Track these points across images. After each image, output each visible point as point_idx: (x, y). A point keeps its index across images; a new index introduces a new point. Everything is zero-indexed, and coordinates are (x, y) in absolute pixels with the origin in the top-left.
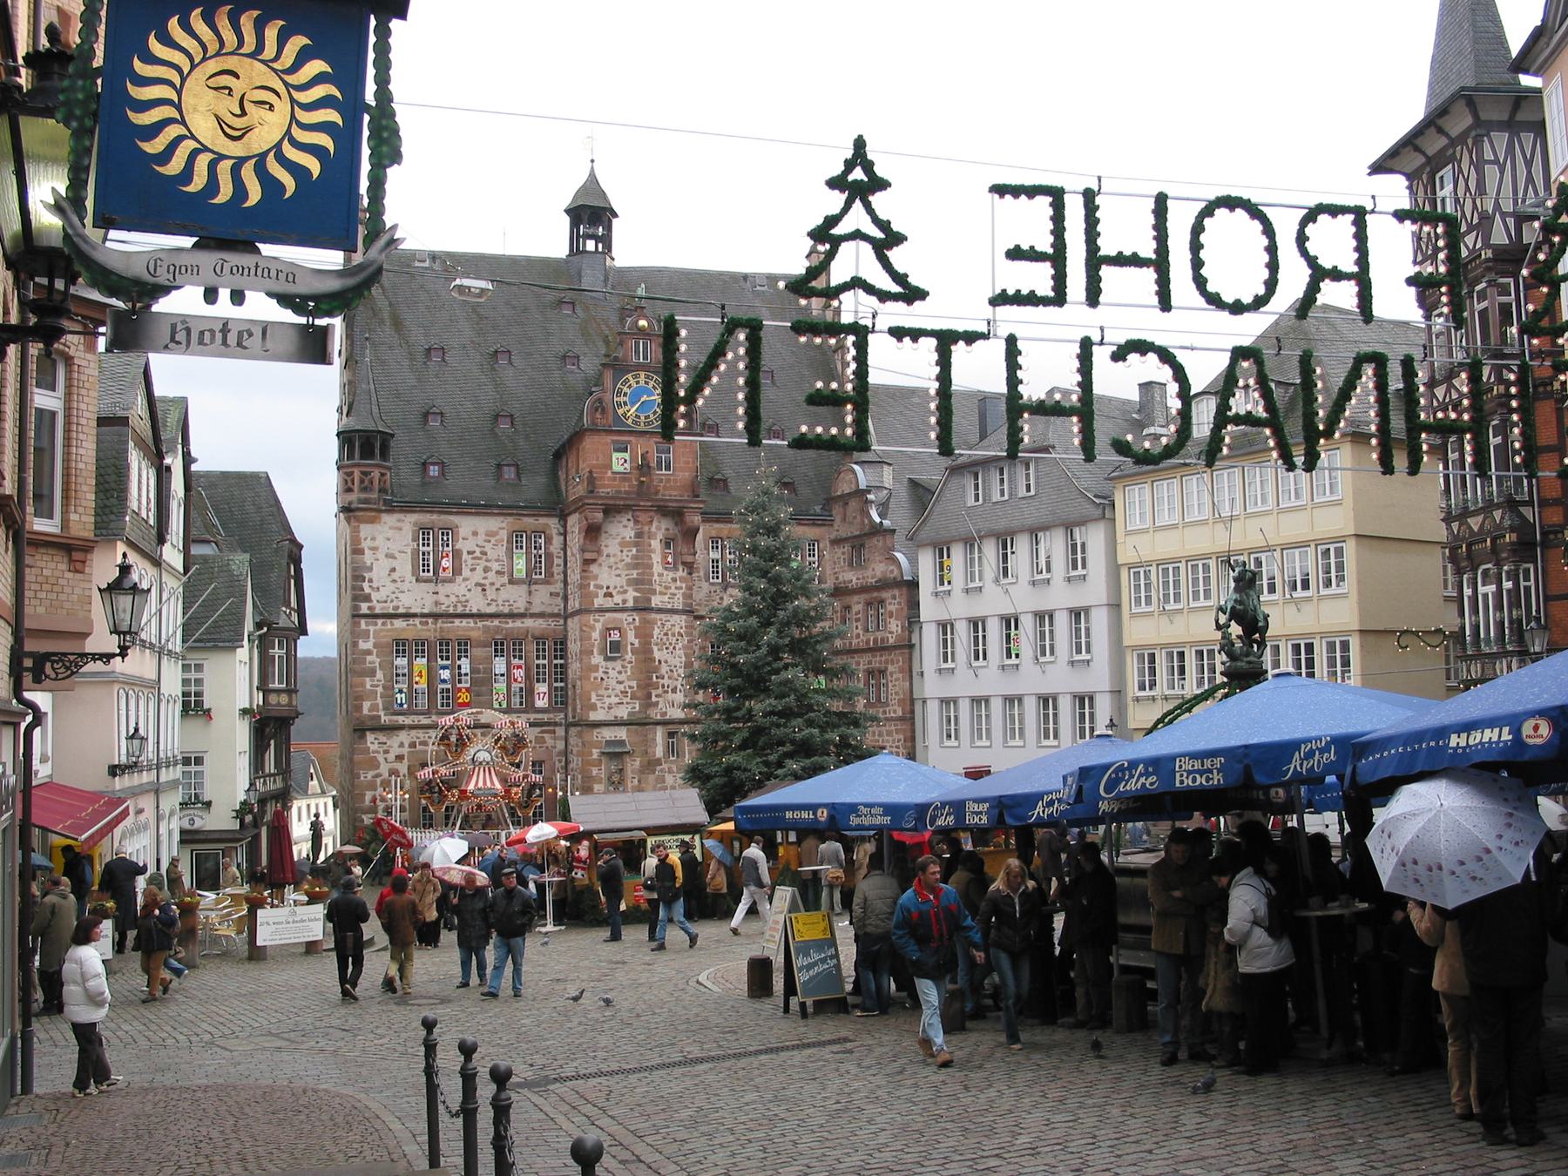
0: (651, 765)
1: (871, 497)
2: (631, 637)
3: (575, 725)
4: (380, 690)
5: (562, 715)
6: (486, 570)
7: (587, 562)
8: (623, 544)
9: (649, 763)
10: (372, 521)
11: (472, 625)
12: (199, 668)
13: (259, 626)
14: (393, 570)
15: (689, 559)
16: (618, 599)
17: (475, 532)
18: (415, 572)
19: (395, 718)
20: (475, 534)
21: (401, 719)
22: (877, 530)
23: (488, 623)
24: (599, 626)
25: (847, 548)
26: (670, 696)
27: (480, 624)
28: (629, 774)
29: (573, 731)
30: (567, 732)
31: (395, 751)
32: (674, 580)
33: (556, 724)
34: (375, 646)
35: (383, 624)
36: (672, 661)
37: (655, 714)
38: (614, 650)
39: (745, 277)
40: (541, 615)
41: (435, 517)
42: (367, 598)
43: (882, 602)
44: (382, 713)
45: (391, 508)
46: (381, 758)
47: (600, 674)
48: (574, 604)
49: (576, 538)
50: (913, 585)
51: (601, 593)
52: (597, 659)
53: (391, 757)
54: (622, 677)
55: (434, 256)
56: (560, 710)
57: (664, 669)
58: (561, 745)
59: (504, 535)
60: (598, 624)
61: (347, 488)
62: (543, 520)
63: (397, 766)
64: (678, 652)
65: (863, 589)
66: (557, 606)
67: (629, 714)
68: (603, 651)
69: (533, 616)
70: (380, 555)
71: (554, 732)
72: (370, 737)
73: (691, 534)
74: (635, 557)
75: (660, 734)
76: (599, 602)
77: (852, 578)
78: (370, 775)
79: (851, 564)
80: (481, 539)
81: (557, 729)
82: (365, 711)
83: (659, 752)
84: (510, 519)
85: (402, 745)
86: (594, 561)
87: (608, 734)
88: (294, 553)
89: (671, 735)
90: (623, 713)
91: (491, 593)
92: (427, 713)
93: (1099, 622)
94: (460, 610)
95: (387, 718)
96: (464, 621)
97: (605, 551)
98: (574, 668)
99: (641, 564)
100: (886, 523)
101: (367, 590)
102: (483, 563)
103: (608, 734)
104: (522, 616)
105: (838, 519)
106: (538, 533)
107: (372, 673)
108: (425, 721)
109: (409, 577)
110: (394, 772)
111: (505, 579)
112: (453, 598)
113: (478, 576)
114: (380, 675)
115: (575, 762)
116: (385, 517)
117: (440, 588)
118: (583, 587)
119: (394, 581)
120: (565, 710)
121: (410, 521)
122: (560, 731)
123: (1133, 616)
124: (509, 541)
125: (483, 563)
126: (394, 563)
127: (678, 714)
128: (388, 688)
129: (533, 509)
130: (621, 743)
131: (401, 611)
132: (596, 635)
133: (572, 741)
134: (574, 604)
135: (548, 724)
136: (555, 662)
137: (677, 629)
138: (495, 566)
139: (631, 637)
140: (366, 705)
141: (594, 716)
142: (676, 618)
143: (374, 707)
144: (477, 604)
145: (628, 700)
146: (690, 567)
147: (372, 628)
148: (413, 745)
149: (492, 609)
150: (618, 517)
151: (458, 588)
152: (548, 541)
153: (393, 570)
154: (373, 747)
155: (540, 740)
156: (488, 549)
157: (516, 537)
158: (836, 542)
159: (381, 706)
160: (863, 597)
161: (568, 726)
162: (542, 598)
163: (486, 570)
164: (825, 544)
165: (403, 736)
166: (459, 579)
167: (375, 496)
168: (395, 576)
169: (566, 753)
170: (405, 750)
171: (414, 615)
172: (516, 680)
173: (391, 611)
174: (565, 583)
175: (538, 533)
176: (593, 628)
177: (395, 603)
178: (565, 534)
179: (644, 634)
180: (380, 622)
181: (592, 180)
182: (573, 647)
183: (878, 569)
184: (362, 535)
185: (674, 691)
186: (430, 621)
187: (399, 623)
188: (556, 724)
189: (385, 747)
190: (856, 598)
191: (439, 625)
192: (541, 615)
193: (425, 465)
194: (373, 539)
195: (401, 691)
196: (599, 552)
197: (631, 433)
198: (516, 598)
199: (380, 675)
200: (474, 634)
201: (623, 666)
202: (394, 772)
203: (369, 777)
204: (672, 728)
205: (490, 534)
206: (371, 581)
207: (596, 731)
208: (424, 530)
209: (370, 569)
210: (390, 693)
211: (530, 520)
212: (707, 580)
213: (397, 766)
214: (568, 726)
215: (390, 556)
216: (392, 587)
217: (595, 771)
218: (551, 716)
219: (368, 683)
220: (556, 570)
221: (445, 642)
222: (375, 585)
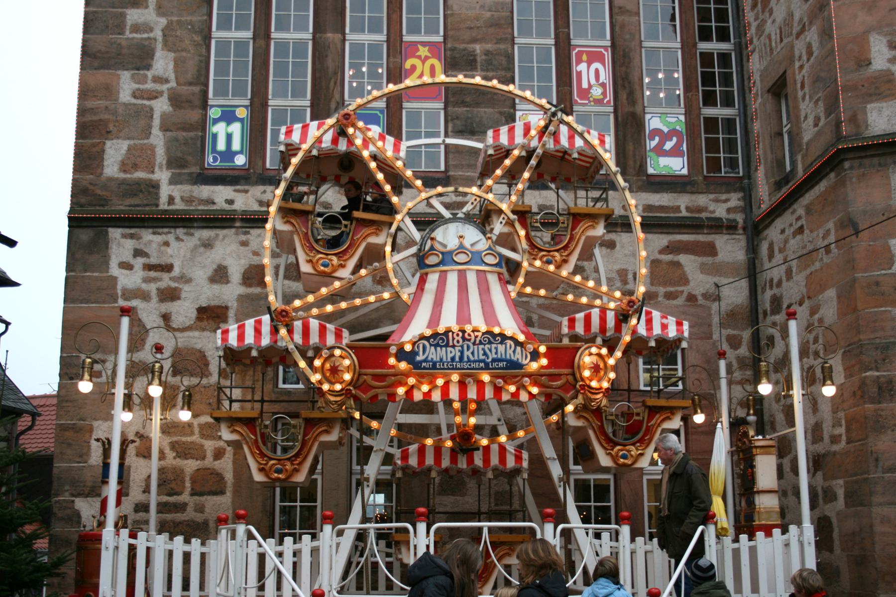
4: (161, 106)
5: (735, 200)
19: (205, 191)
30: (753, 249)
33: (717, 226)
44: (162, 176)
56: (729, 185)
71: (710, 250)
81: (721, 241)
85: (220, 275)
95: (178, 191)
120: (746, 187)
133: (773, 271)
135: (693, 225)
136: (704, 46)
154: (128, 280)
172: (585, 93)
188: (717, 226)
189: (166, 281)
195: (229, 117)
210: (194, 115)
218: (702, 200)
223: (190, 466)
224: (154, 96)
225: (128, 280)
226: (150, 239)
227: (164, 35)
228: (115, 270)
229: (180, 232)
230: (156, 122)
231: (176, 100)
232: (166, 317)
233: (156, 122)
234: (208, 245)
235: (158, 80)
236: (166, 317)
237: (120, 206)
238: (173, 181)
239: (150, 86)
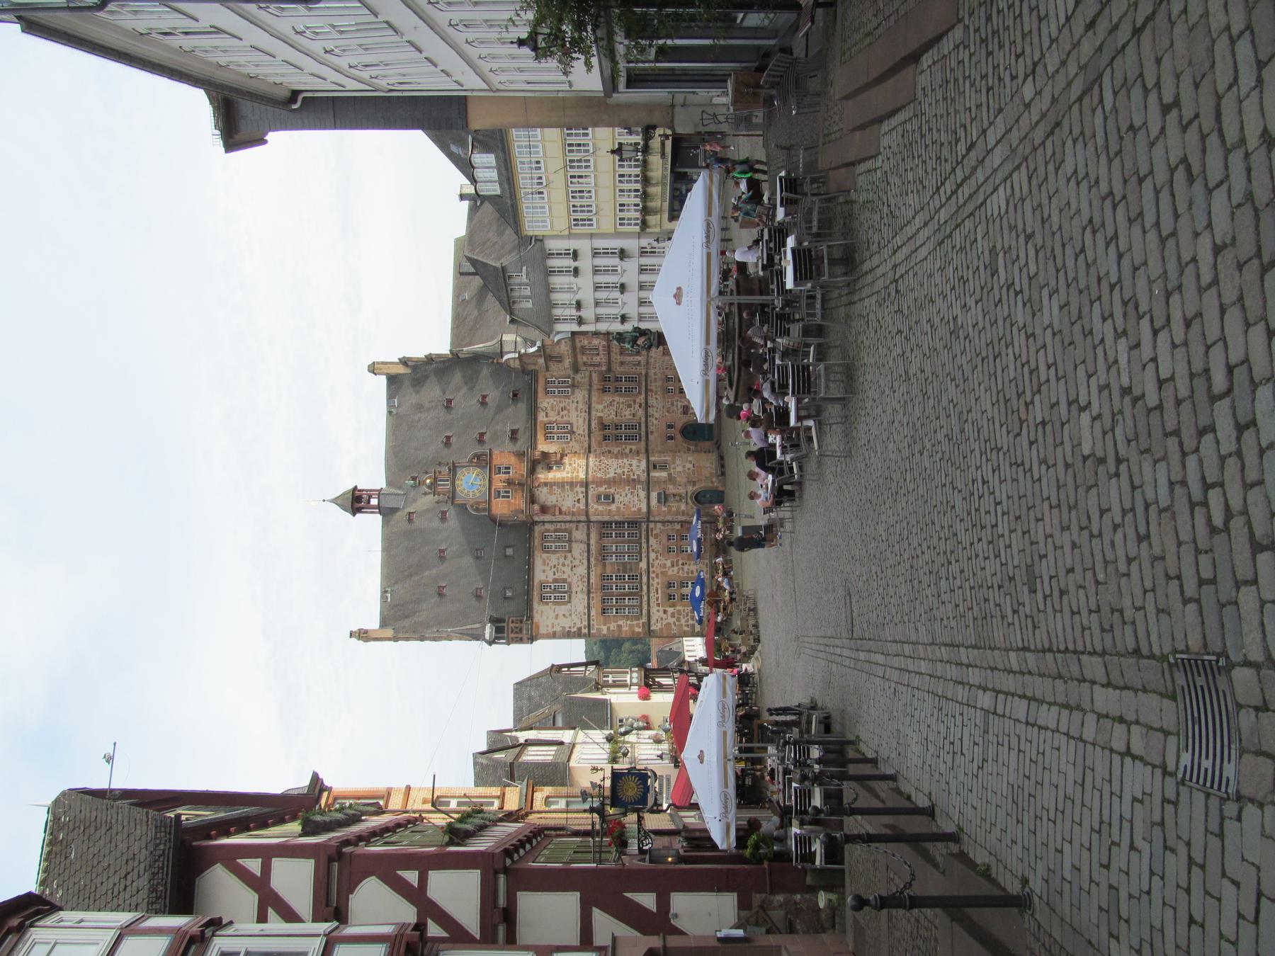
0: (671, 479)
1: (523, 351)
2: (602, 489)
3: (648, 518)
6: (564, 565)
7: (561, 512)
8: (551, 493)
9: (670, 480)
10: (538, 627)
12: (621, 721)
13: (597, 689)
15: (559, 456)
16: (581, 496)
17: (545, 569)
18: (565, 603)
20: (544, 571)
21: (644, 611)
22: (543, 347)
24: (595, 506)
25: (551, 364)
26: (634, 467)
28: (676, 491)
29: (651, 519)
32: (570, 464)
33: (648, 527)
36: (615, 466)
37: (643, 477)
38: (609, 498)
39: (390, 413)
40: (588, 535)
41: (535, 593)
42: (580, 629)
43: (583, 347)
45: (530, 617)
46: (665, 622)
47: (622, 506)
48: (583, 518)
49: (547, 518)
50: (573, 333)
51: (577, 505)
52: (613, 507)
53: (665, 616)
55: (384, 592)
57: (619, 471)
58: (659, 525)
59: (545, 556)
60: (594, 507)
61: (521, 641)
62: (536, 534)
63: (669, 614)
64: (610, 463)
65: (575, 356)
66: (583, 526)
68: (609, 504)
69: (589, 540)
70: (556, 622)
73: (545, 455)
74: (558, 487)
75: (654, 474)
76: (582, 506)
77: (567, 362)
79: (560, 361)
80: (547, 568)
82: (640, 630)
83: (664, 474)
84: (536, 552)
86: (560, 509)
87: (654, 502)
88: (556, 669)
89: (655, 467)
90: (643, 494)
91: (576, 562)
92: (641, 597)
93: (601, 244)
94: (586, 580)
97: (555, 503)
98: (617, 518)
99: (562, 484)
100: (539, 344)
101: (575, 629)
102: (560, 567)
103: (654, 502)
104: (589, 545)
105: (533, 367)
106: (544, 537)
107: (620, 626)
108: (645, 599)
110: (673, 615)
111: (569, 555)
112: (580, 583)
113: (567, 570)
114: (620, 622)
115: (669, 518)
116: (535, 620)
117: (574, 590)
118: (573, 514)
120: (640, 522)
121: (537, 607)
122: (652, 525)
123: (598, 227)
124: (548, 552)
125: (560, 567)
126: (561, 615)
127: (643, 464)
128: (627, 618)
129: (530, 539)
130: (659, 495)
132: (600, 508)
133: (657, 519)
134: (583, 518)
137: (597, 463)
138: (562, 560)
139: (602, 489)
140: (638, 630)
141: (644, 509)
142: (591, 463)
143: (638, 626)
144: (582, 570)
146: (563, 456)
147: (596, 627)
148: (658, 605)
149: (585, 562)
150: (536, 495)
151: (574, 580)
152: (548, 531)
155: (656, 536)
156: (552, 564)
157: (545, 549)
158: (547, 369)
160: (579, 356)
161: (648, 521)
162: (579, 534)
163: (564, 565)
164: (548, 375)
165: (654, 610)
166: (569, 580)
167: (524, 627)
168: (567, 614)
169: (663, 522)
170: (661, 609)
171: (589, 604)
174: (570, 522)
175: (544, 537)
176: (596, 510)
178: (544, 522)
179: (600, 483)
181: (335, 501)
182: (606, 518)
183: (565, 349)
184: (545, 632)
185: (631, 465)
187: (593, 612)
188: (648, 527)
190: (579, 360)
192: (588, 535)
193: (506, 598)
196: (555, 506)
197: (490, 489)
198: (578, 549)
199: (620, 622)
200: (599, 572)
202: (673, 615)
204: (651, 467)
205: (544, 563)
207: (652, 508)
208: (542, 598)
209: (564, 628)
211: (536, 541)
212: (568, 443)
213: (669, 614)
214: (648, 521)
216: (573, 616)
217: (674, 509)
219: (625, 628)
220: (563, 527)
221: (603, 588)
225: (659, 625)
226: (652, 623)
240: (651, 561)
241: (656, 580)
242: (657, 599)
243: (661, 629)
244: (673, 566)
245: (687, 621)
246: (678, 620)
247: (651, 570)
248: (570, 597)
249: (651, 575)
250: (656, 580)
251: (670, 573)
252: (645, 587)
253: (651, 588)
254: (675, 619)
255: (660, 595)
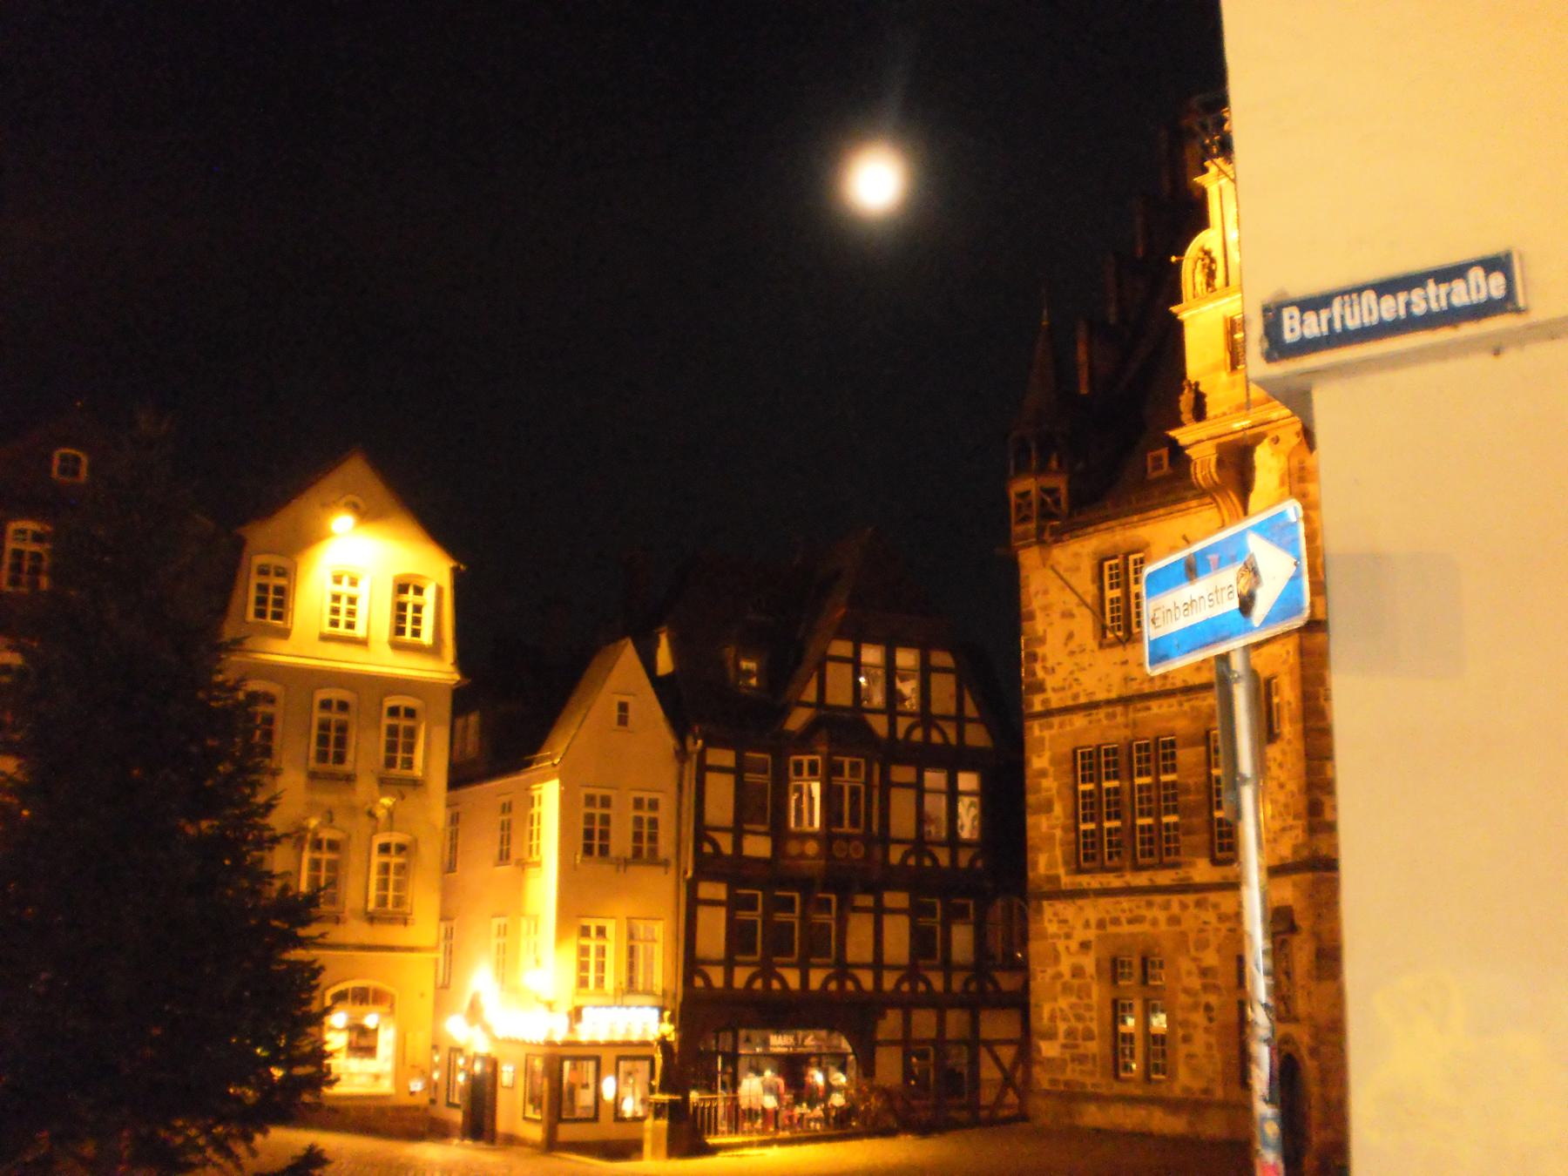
4: (1058, 833)
11: (1175, 709)
14: (1070, 636)
23: (1196, 703)
27: (1186, 706)
31: (1080, 935)
34: (1053, 761)
35: (1061, 725)
44: (1061, 871)
46: (1061, 946)
53: (1074, 945)
54: (1283, 777)
67: (1296, 849)
70: (1055, 617)
72: (1048, 908)
78: (1050, 971)
85: (1087, 925)
96: (1165, 702)
101: (1040, 674)
107: (1047, 807)
109: (1091, 644)
110: (1077, 972)
114: (1058, 809)
119: (1072, 653)
131: (1083, 700)
143: (1051, 864)
145: (1290, 821)
147: (1047, 734)
148: (1101, 924)
153: (1070, 636)
154: (1052, 928)
159: (1060, 860)
165: (1093, 910)
168: (1073, 646)
170: (1091, 934)
173: (1070, 703)
177: (1076, 689)
180: (1056, 720)
186: (1119, 709)
187: (1079, 721)
191: (1131, 715)
194: (1046, 592)
199: (1058, 809)
200: (1182, 725)
201: (1284, 753)
202: (1077, 972)
203: (1047, 979)
206: (1044, 659)
209: (1042, 641)
215: (1067, 615)
216: (1068, 664)
222: (1049, 664)
223: (1080, 1026)
224: (1053, 827)
226: (1060, 906)
227: (1058, 793)
228: (1046, 924)
229: (1070, 901)
230: (1057, 842)
231: (1064, 829)
232: (1067, 948)
233: (1057, 842)
234: (1081, 908)
235: (1057, 818)
236: (1067, 948)
237: (1047, 888)
238: (1067, 874)
239: (1054, 822)
240: (1213, 897)
241: (1162, 916)
242: (1116, 921)
243: (1043, 936)
244: (1204, 972)
245: (1065, 1019)
246: (1067, 989)
247: (1190, 898)
248: (1111, 645)
249: (1175, 900)
250: (1162, 916)
251: (1185, 965)
252: (1142, 879)
253: (1141, 900)
254: (1067, 976)
255: (1126, 929)
